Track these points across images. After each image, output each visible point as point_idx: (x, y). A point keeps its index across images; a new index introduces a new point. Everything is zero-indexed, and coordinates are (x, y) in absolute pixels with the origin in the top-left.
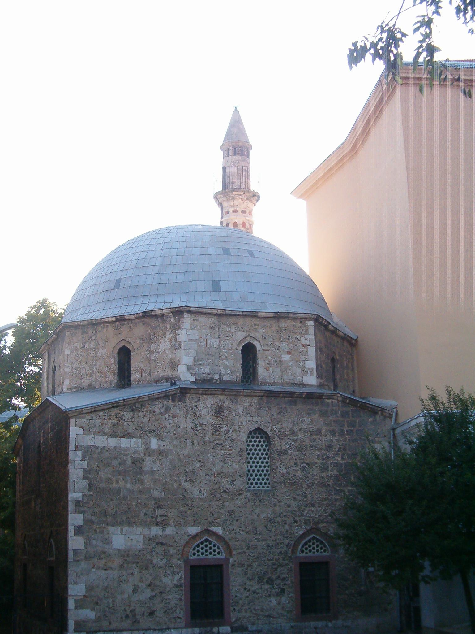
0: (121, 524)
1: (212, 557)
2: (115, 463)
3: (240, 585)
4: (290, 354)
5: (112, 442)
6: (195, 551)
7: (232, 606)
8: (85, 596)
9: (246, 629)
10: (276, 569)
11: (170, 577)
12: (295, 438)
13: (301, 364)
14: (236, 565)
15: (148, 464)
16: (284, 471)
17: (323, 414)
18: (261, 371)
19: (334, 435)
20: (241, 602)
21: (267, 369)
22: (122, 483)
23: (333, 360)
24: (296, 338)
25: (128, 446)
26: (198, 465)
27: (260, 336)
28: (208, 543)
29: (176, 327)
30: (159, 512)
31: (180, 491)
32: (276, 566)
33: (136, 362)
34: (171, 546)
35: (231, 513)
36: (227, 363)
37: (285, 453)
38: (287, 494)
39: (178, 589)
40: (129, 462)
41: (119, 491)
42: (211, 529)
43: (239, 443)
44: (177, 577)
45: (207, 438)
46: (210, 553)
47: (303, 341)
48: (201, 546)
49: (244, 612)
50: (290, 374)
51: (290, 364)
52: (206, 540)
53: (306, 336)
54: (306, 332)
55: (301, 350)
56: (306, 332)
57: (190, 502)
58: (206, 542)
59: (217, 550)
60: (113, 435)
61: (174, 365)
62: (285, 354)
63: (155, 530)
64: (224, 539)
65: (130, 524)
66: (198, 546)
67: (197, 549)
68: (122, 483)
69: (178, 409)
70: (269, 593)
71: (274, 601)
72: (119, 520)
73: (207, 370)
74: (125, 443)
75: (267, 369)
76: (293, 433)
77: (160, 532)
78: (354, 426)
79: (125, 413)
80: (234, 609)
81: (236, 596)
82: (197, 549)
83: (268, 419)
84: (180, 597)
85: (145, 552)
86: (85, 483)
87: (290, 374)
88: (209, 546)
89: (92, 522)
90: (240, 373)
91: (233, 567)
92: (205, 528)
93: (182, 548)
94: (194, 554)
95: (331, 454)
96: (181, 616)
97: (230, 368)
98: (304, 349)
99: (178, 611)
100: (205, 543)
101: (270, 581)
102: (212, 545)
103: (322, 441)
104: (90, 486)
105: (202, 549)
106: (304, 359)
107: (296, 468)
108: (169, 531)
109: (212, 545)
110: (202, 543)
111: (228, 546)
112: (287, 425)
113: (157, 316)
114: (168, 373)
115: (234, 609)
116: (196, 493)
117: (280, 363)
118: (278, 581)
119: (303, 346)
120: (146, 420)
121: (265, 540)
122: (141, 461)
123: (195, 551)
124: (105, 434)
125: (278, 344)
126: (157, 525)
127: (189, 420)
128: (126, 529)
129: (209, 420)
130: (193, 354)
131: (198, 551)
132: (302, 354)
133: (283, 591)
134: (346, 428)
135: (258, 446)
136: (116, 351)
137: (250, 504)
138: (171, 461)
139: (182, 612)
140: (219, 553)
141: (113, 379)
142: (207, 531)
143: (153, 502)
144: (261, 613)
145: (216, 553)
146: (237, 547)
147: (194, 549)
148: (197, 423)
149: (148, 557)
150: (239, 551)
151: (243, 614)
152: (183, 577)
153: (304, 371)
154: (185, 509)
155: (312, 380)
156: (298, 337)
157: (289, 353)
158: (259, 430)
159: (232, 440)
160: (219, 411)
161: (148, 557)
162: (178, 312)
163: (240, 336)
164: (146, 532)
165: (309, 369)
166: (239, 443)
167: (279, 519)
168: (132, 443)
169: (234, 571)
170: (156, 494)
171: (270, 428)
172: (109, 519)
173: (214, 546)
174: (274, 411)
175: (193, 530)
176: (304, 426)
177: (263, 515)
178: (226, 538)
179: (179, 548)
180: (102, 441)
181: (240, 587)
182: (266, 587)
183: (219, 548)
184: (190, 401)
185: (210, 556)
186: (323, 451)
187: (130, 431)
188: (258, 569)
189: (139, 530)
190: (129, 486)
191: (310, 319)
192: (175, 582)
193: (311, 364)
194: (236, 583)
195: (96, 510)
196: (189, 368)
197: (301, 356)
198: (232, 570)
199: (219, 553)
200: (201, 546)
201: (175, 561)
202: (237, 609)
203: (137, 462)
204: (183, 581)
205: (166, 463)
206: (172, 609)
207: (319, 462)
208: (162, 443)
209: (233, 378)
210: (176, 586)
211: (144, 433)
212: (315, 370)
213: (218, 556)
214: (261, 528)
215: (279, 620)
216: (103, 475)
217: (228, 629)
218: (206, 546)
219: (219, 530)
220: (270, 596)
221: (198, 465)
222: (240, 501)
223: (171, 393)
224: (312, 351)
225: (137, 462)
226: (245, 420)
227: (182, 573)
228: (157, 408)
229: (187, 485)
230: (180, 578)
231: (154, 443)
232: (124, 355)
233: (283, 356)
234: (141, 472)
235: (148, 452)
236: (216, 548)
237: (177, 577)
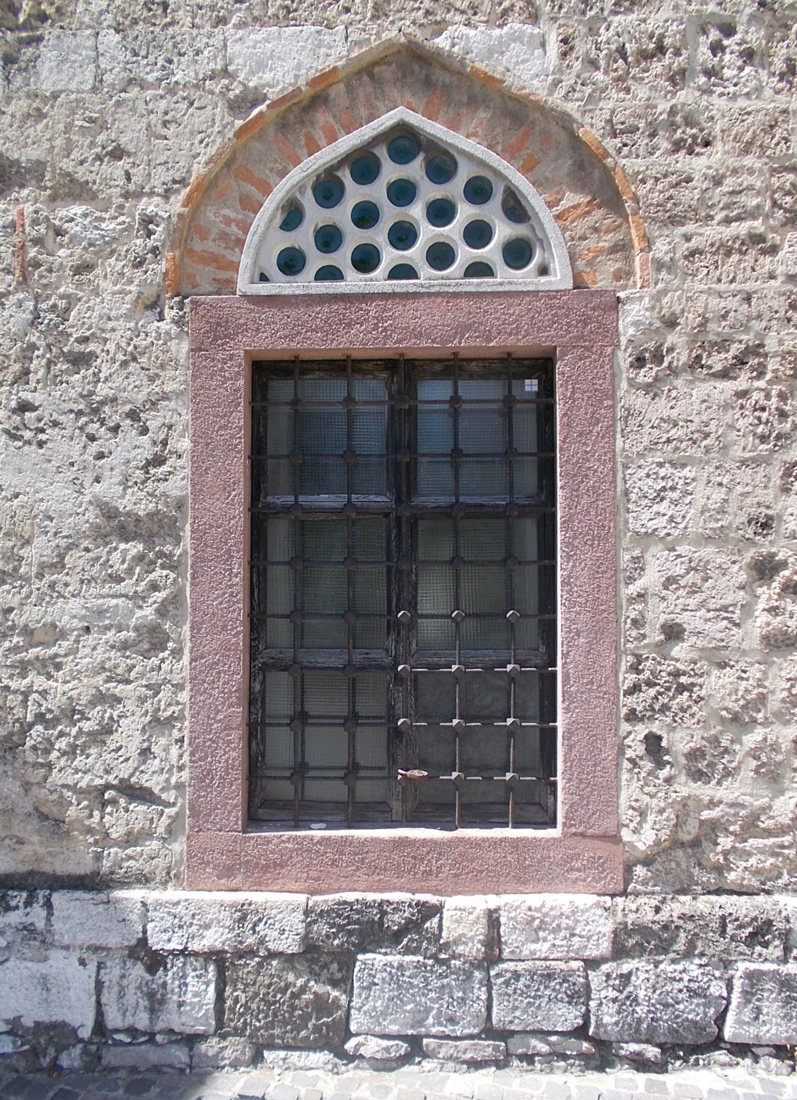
3: (718, 538)
6: (303, 238)
7: (632, 716)
14: (682, 357)
20: (718, 685)
28: (415, 170)
34: (75, 190)
39: (135, 548)
42: (442, 42)
44: (131, 448)
48: (355, 194)
49: (747, 772)
52: (404, 142)
58: (401, 156)
59: (503, 231)
64: (565, 122)
80: (653, 743)
81: (673, 632)
84: (148, 613)
88: (429, 191)
91: (645, 375)
92: (391, 33)
93: (177, 205)
94: (291, 263)
96: (154, 783)
99: (129, 734)
100: (391, 172)
102: (455, 189)
109: (455, 189)
110: (363, 165)
111: (608, 194)
115: (653, 743)
139: (170, 750)
140: (518, 253)
142: (416, 66)
145: (491, 252)
146: (688, 196)
150: (714, 232)
151: (737, 791)
152: (185, 444)
169: (661, 407)
175: (284, 58)
178: (591, 130)
179: (150, 206)
181: (708, 552)
183: (516, 210)
192: (109, 489)
198: (639, 401)
199: (518, 253)
200: (355, 194)
201: (106, 305)
202: (680, 742)
204: (178, 485)
206: (71, 713)
210: (116, 525)
218: (402, 193)
227: (179, 413)
230: (158, 461)
236: (491, 211)
237: (131, 448)
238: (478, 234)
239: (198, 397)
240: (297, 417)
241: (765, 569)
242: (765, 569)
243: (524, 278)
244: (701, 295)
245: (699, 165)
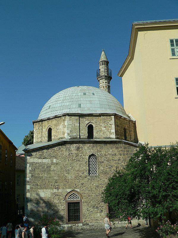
0: (43, 188)
1: (75, 200)
2: (41, 168)
3: (86, 209)
5: (40, 161)
8: (30, 213)
9: (88, 224)
10: (99, 203)
11: (60, 207)
12: (107, 157)
15: (52, 168)
16: (102, 169)
17: (117, 148)
18: (95, 134)
19: (121, 155)
21: (97, 133)
22: (43, 174)
23: (125, 130)
25: (45, 162)
26: (71, 167)
27: (94, 122)
29: (64, 120)
30: (56, 184)
31: (64, 177)
32: (99, 202)
33: (53, 133)
34: (60, 196)
35: (82, 184)
36: (82, 132)
37: (103, 162)
38: (103, 177)
40: (46, 167)
41: (42, 177)
43: (86, 159)
44: (63, 207)
45: (74, 158)
46: (75, 198)
47: (110, 123)
48: (72, 196)
57: (67, 181)
60: (40, 158)
61: (64, 134)
63: (55, 191)
65: (46, 188)
66: (71, 196)
67: (70, 197)
68: (43, 174)
69: (63, 148)
70: (97, 212)
71: (99, 215)
72: (42, 187)
73: (75, 135)
74: (44, 161)
75: (97, 133)
76: (105, 155)
77: (57, 191)
78: (129, 152)
79: (44, 150)
82: (70, 197)
83: (96, 151)
85: (51, 198)
86: (30, 175)
89: (33, 188)
90: (87, 135)
94: (69, 198)
95: (120, 162)
97: (84, 134)
101: (97, 208)
103: (117, 158)
104: (32, 176)
105: (72, 197)
107: (107, 168)
108: (60, 191)
110: (72, 195)
112: (103, 152)
113: (59, 117)
114: (62, 136)
116: (70, 178)
117: (101, 131)
118: (100, 208)
120: (52, 152)
121: (96, 193)
122: (50, 167)
123: (69, 198)
124: (37, 158)
126: (56, 189)
127: (67, 152)
128: (45, 190)
129: (75, 152)
130: (70, 129)
131: (71, 197)
133: (102, 211)
134: (125, 153)
135: (93, 160)
136: (48, 130)
137: (89, 181)
138: (61, 167)
140: (78, 198)
141: (47, 139)
143: (54, 181)
144: (94, 219)
147: (69, 197)
148: (70, 153)
149: (53, 200)
151: (87, 219)
153: (111, 133)
154: (66, 183)
155: (113, 136)
158: (93, 155)
159: (83, 159)
160: (78, 149)
161: (53, 200)
162: (64, 115)
163: (87, 122)
164: (52, 191)
166: (86, 159)
167: (100, 186)
168: (47, 161)
170: (55, 178)
171: (97, 154)
172: (39, 187)
173: (77, 195)
174: (98, 148)
175: (69, 190)
176: (109, 153)
177: (94, 185)
180: (36, 160)
182: (96, 209)
183: (78, 196)
184: (68, 146)
185: (75, 199)
186: (117, 161)
187: (46, 156)
188: (93, 203)
189: (49, 190)
190: (46, 175)
191: (113, 115)
193: (113, 131)
194: (84, 209)
195: (34, 184)
196: (68, 134)
199: (78, 198)
200: (72, 196)
201: (62, 201)
202: (85, 217)
203: (49, 167)
205: (59, 167)
207: (115, 165)
208: (57, 160)
209: (85, 137)
211: (51, 157)
212: (115, 133)
213: (78, 199)
214: (94, 189)
215: (101, 221)
216: (37, 171)
217: (82, 224)
218: (74, 196)
219: (78, 190)
220: (97, 213)
221: (71, 167)
222: (86, 179)
223: (60, 143)
224: (113, 126)
225: (49, 167)
226: (88, 151)
228: (56, 148)
229: (67, 175)
231: (55, 161)
232: (50, 131)
234: (50, 170)
235: (52, 163)
237: (63, 207)
238: (77, 197)
239: (66, 204)
240: (70, 204)
241: (88, 210)
242: (88, 210)
243: (78, 199)
244: (85, 200)
245: (85, 195)
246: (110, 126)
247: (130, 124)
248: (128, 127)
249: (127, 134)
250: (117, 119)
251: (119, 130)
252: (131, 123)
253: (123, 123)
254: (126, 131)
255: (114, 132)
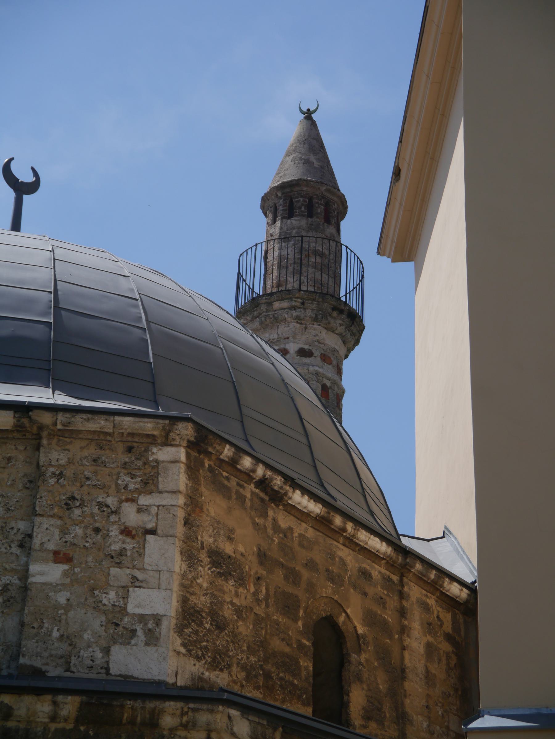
4: (68, 559)
13: (111, 597)
24: (100, 504)
47: (131, 516)
50: (56, 634)
51: (62, 598)
53: (144, 500)
54: (150, 484)
55: (116, 547)
56: (145, 483)
62: (45, 561)
87: (56, 634)
98: (130, 545)
106: (125, 580)
119: (126, 532)
125: (22, 525)
132: (119, 565)
153: (121, 627)
156: (111, 501)
157: (59, 557)
165: (142, 618)
197: (114, 571)
233: (34, 568)
246: (122, 553)
247: (402, 595)
248: (371, 619)
249: (357, 698)
250: (223, 490)
251: (238, 611)
252: (415, 591)
253: (311, 565)
254: (342, 661)
255: (158, 619)
